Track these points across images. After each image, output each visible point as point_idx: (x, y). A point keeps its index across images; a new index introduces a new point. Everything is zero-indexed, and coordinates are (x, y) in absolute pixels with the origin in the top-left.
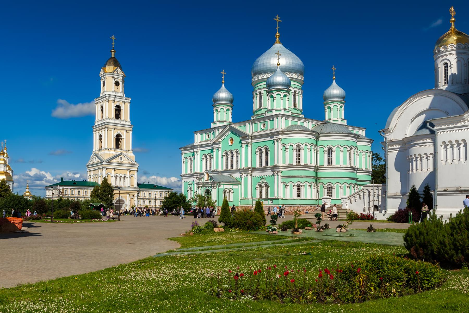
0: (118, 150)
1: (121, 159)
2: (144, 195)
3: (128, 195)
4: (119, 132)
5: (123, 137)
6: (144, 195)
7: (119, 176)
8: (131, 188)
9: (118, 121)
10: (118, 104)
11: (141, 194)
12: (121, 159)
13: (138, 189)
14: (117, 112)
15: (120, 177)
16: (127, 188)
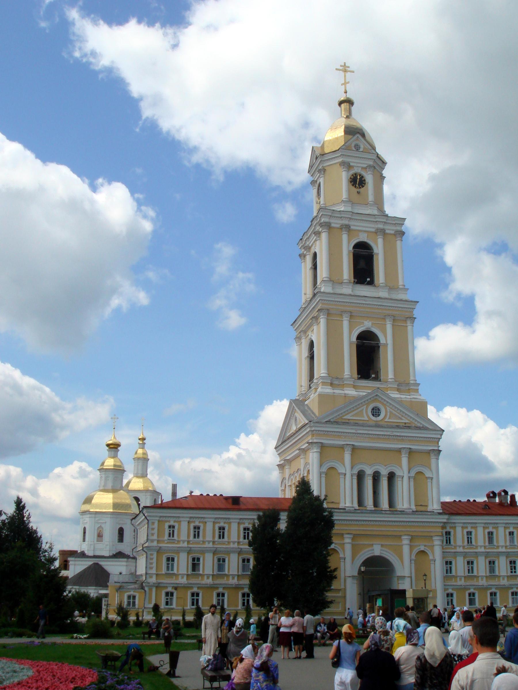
0: (364, 383)
1: (376, 412)
2: (469, 541)
3: (405, 541)
4: (367, 325)
5: (382, 340)
6: (469, 541)
7: (369, 471)
8: (414, 512)
9: (364, 290)
10: (363, 238)
11: (459, 536)
12: (376, 412)
13: (444, 519)
14: (362, 264)
15: (376, 477)
16: (402, 512)
